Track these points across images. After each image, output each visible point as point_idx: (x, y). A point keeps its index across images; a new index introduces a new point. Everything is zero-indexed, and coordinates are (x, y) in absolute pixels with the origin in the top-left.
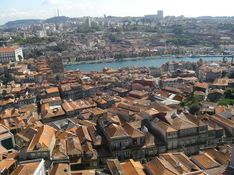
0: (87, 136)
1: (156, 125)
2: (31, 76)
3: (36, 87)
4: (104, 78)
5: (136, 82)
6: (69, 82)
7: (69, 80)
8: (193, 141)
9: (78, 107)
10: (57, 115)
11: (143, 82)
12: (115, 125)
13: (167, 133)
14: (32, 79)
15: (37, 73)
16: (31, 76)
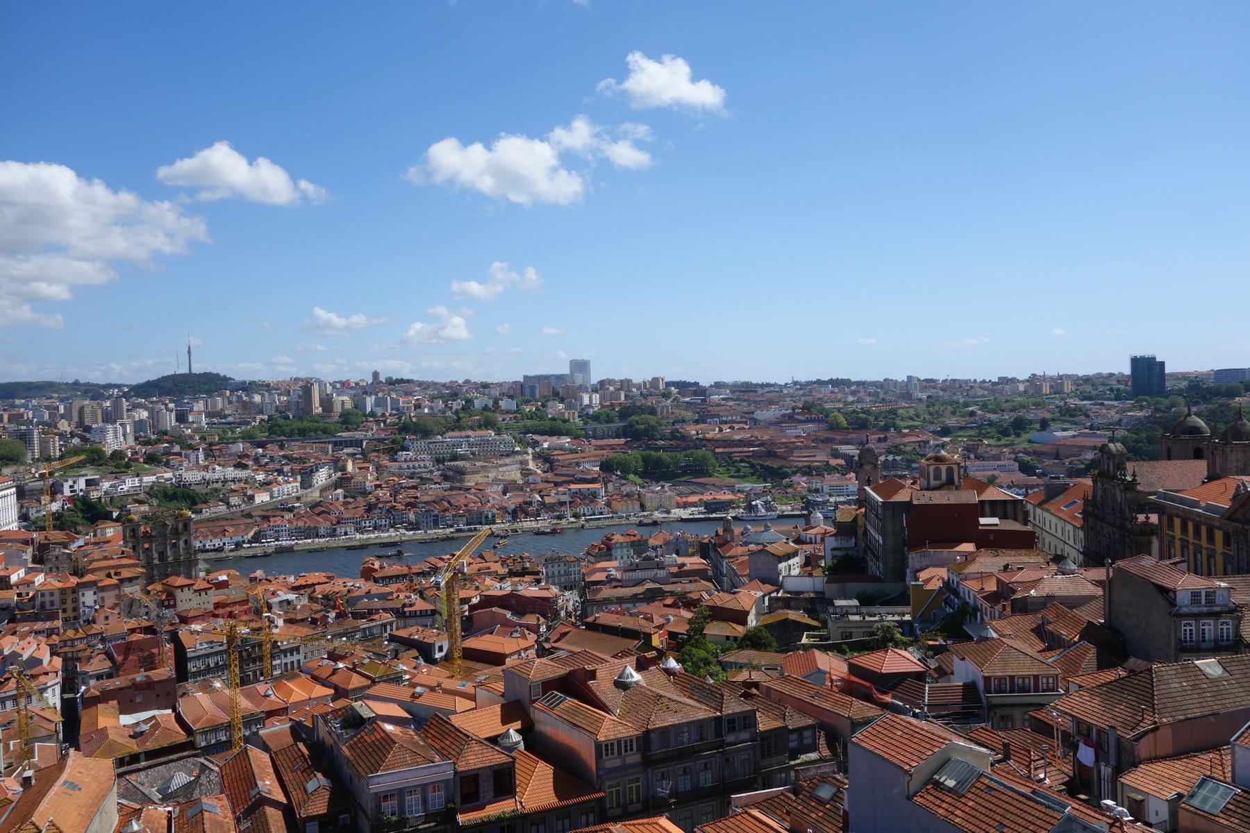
0: (268, 784)
1: (555, 718)
2: (47, 594)
3: (65, 638)
4: (361, 597)
5: (487, 601)
6: (216, 616)
7: (217, 605)
8: (707, 779)
9: (245, 704)
10: (150, 746)
11: (513, 602)
12: (389, 727)
13: (598, 746)
14: (48, 606)
15: (74, 580)
16: (47, 594)
